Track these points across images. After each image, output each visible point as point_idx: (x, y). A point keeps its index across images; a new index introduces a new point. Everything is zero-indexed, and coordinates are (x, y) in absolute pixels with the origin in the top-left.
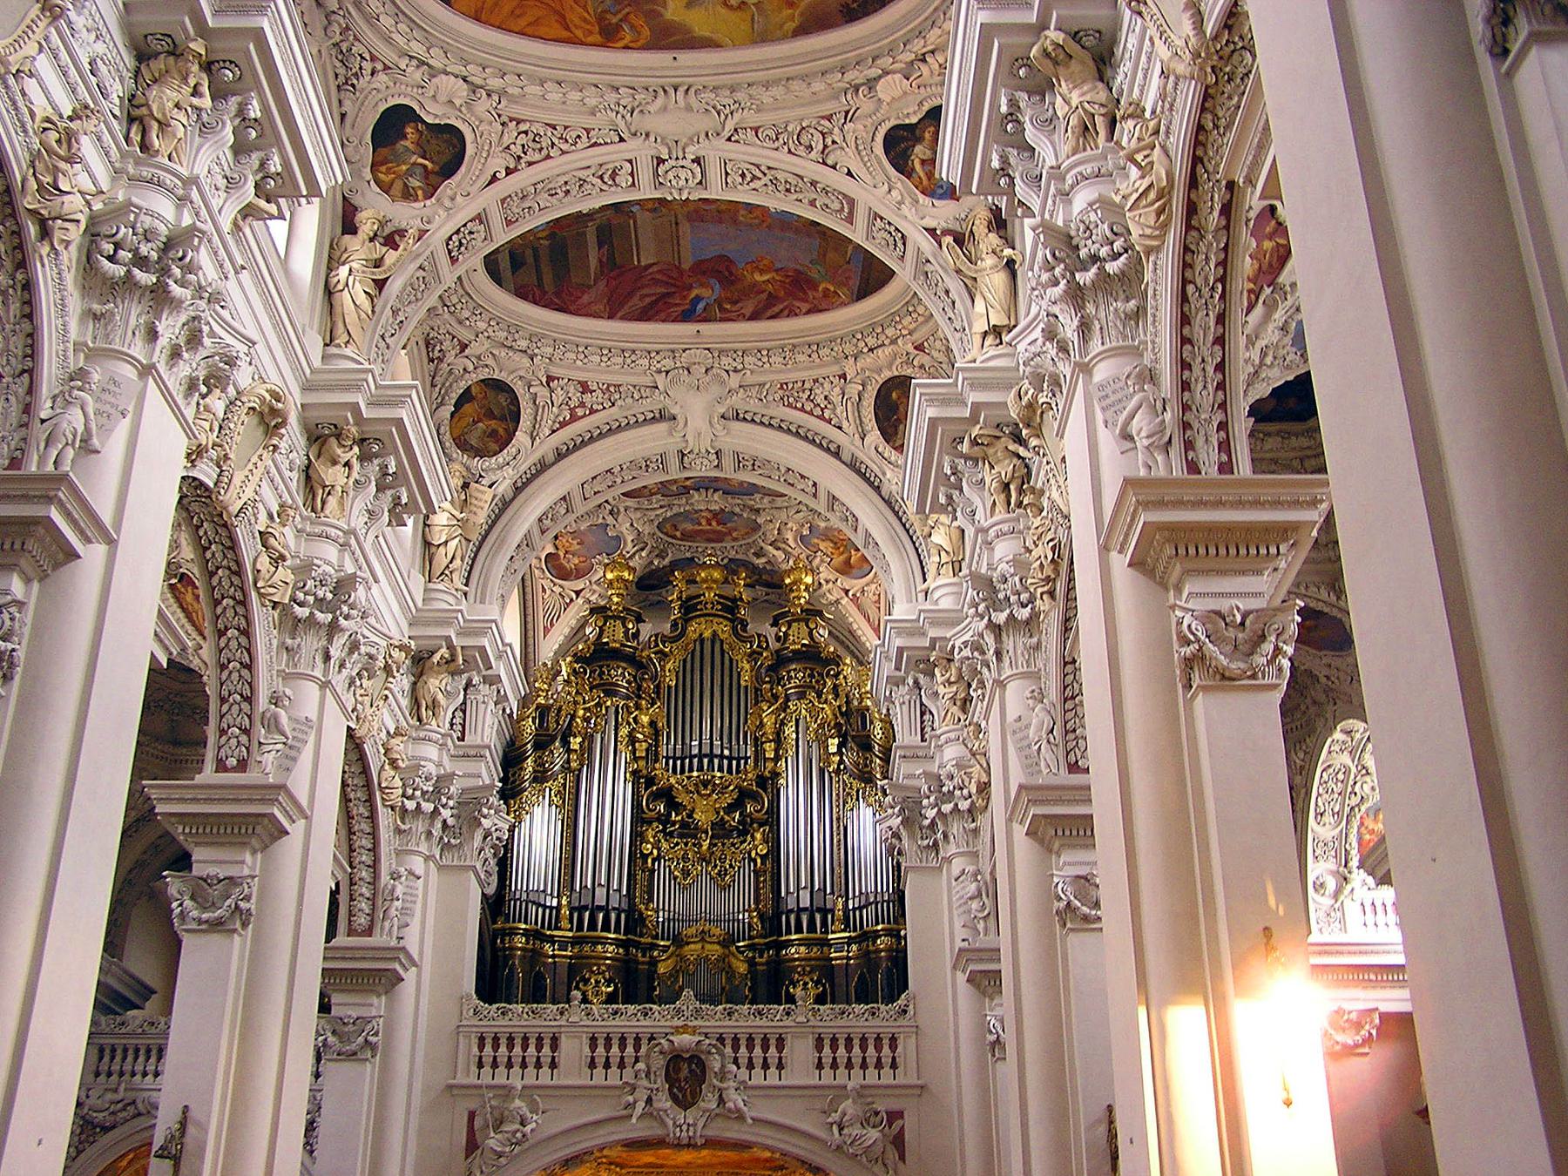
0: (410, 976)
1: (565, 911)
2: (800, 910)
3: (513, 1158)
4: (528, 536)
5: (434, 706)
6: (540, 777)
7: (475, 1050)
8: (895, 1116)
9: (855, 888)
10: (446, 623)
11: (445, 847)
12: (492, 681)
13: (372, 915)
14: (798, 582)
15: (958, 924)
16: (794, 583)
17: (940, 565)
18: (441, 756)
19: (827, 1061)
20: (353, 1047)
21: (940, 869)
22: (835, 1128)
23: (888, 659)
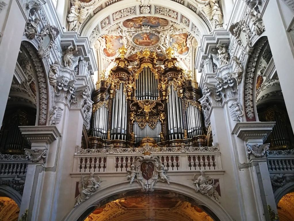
1: (109, 135)
2: (174, 133)
3: (91, 196)
4: (97, 26)
5: (69, 63)
6: (102, 99)
7: (79, 163)
8: (217, 181)
9: (189, 127)
10: (72, 37)
11: (72, 104)
12: (87, 59)
16: (169, 53)
17: (216, 25)
18: (71, 77)
19: (192, 164)
20: (37, 159)
21: (223, 107)
22: (197, 185)
23: (203, 51)
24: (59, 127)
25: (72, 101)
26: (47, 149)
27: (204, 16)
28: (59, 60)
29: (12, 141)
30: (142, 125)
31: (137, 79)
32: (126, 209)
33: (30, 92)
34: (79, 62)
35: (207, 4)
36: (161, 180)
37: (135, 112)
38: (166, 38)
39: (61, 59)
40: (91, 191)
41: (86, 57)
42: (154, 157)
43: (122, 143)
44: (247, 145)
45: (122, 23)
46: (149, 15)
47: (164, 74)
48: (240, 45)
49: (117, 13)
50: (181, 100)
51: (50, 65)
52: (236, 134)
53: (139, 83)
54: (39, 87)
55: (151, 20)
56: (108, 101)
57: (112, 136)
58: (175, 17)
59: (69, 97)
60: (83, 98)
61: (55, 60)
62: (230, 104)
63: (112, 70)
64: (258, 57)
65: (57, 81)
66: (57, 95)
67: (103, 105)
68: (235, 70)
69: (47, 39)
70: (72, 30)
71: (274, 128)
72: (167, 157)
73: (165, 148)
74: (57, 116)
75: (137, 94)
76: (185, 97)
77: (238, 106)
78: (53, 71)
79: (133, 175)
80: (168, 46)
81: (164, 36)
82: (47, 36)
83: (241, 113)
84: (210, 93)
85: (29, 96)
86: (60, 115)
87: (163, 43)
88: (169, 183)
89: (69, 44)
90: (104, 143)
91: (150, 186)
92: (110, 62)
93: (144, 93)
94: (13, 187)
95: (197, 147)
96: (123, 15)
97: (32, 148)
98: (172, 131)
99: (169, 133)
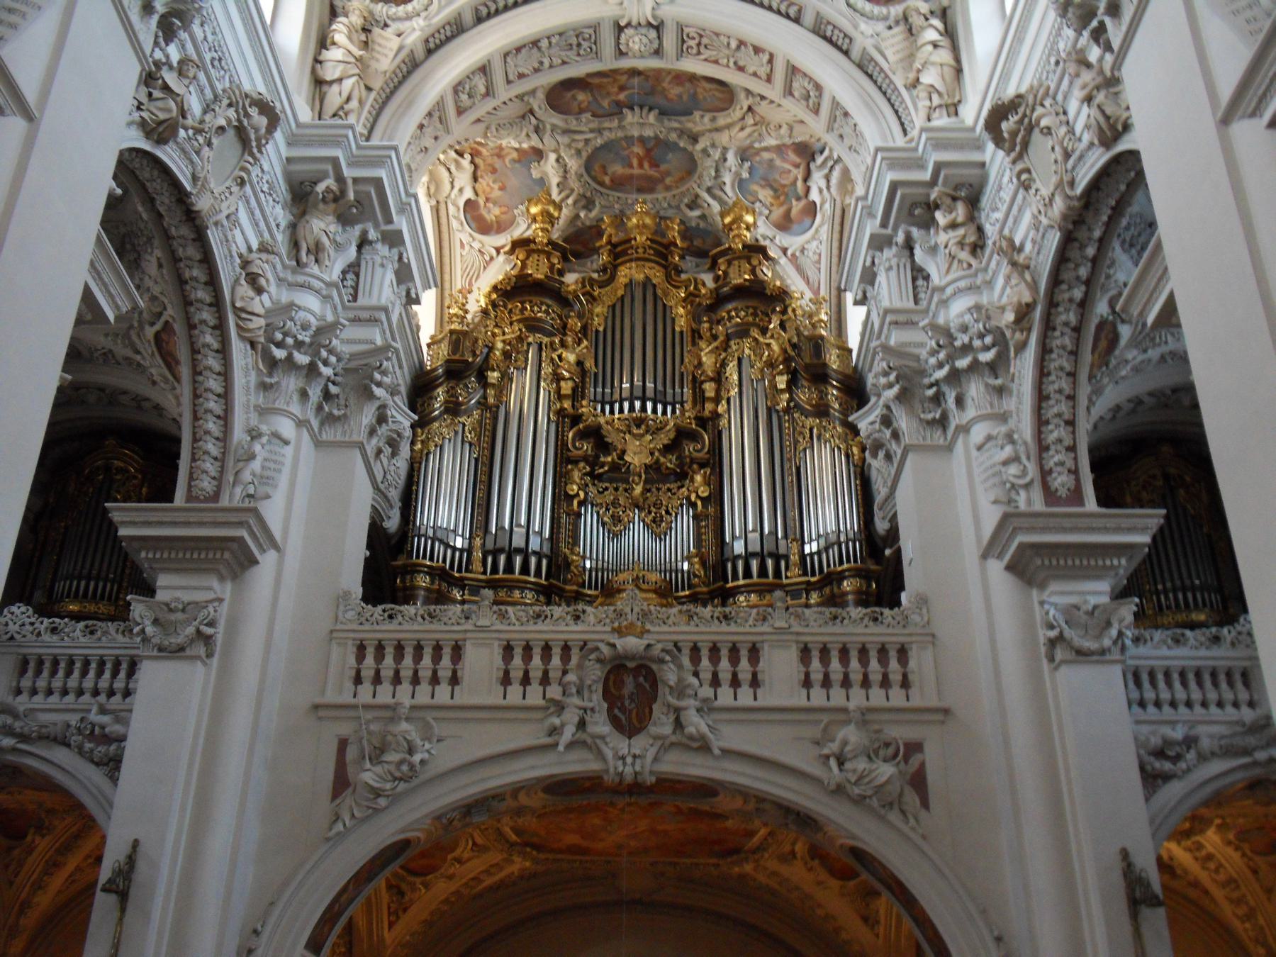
0: (268, 560)
2: (748, 556)
3: (395, 798)
4: (440, 104)
5: (317, 250)
6: (453, 409)
7: (352, 661)
8: (914, 747)
9: (811, 530)
12: (394, 239)
13: (219, 479)
14: (738, 220)
15: (985, 501)
17: (931, 109)
19: (817, 676)
20: (180, 640)
21: (950, 448)
23: (872, 215)
24: (273, 512)
25: (326, 409)
26: (221, 600)
27: (882, 70)
28: (280, 237)
29: (82, 567)
30: (617, 520)
31: (601, 329)
32: (542, 856)
33: (157, 368)
34: (360, 247)
35: (897, 23)
36: (684, 740)
37: (587, 462)
38: (725, 160)
39: (288, 233)
40: (398, 774)
41: (389, 227)
42: (660, 646)
43: (531, 589)
44: (1042, 603)
45: (541, 95)
46: (654, 63)
47: (712, 308)
48: (1027, 188)
49: (524, 51)
50: (779, 418)
51: (241, 256)
52: (1000, 556)
53: (606, 344)
54: (192, 344)
55: (665, 85)
56: (476, 413)
57: (490, 559)
58: (763, 71)
59: (315, 393)
60: (371, 396)
61: (262, 236)
62: (979, 432)
63: (495, 288)
64: (1101, 240)
65: (267, 325)
66: (268, 380)
67: (456, 433)
68: (1005, 292)
69: (227, 145)
70: (334, 115)
71: (1159, 539)
72: (714, 650)
73: (707, 611)
74: (263, 467)
75: (599, 390)
76: (797, 406)
77: (1013, 442)
78: (253, 279)
79: (571, 717)
80: (730, 193)
81: (717, 155)
82: (231, 133)
83: (1024, 472)
84: (896, 389)
85: (154, 383)
86: (275, 462)
87: (709, 184)
88: (717, 752)
89: (318, 171)
90: (456, 586)
91: (638, 761)
92: (492, 258)
93: (626, 386)
94: (80, 751)
95: (840, 611)
96: (546, 62)
97: (161, 596)
98: (739, 548)
99: (727, 554)
